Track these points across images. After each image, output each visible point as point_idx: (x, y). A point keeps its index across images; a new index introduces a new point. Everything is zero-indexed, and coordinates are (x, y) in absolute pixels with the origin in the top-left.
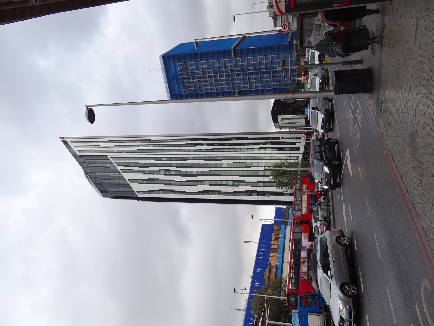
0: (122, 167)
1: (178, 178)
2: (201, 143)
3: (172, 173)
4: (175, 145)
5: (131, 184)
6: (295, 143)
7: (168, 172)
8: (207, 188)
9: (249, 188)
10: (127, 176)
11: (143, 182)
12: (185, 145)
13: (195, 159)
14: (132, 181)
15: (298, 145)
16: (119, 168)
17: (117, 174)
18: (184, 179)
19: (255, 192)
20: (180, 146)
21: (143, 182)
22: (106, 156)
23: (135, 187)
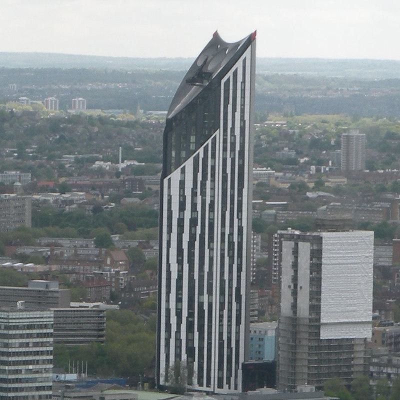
0: (201, 156)
1: (186, 238)
2: (229, 235)
3: (193, 229)
4: (232, 226)
5: (179, 169)
6: (229, 382)
7: (193, 222)
8: (174, 276)
9: (174, 328)
10: (189, 164)
11: (182, 184)
12: (231, 243)
13: (211, 259)
14: (183, 171)
15: (226, 386)
16: (201, 151)
17: (192, 147)
18: (185, 246)
19: (170, 336)
20: (231, 234)
21: (182, 184)
22: (219, 128)
23: (176, 176)
